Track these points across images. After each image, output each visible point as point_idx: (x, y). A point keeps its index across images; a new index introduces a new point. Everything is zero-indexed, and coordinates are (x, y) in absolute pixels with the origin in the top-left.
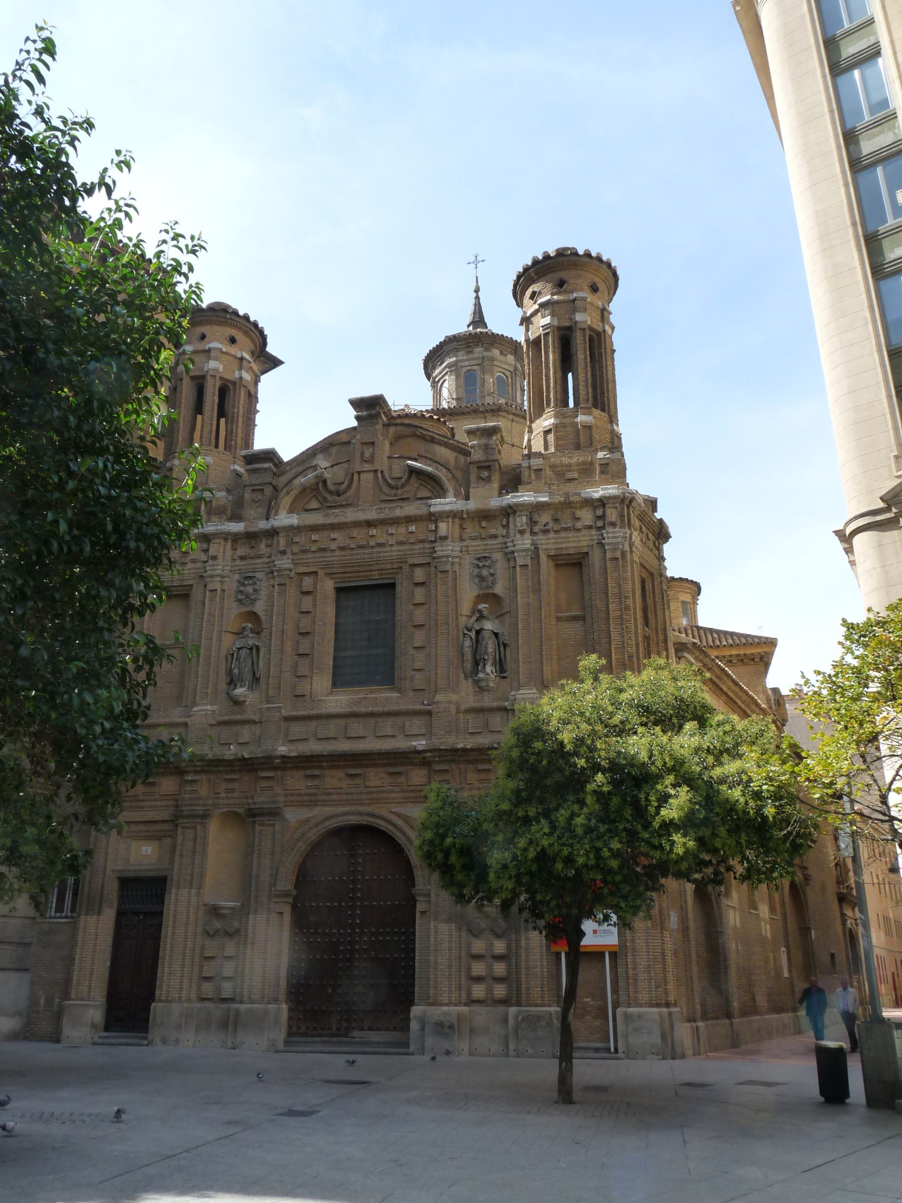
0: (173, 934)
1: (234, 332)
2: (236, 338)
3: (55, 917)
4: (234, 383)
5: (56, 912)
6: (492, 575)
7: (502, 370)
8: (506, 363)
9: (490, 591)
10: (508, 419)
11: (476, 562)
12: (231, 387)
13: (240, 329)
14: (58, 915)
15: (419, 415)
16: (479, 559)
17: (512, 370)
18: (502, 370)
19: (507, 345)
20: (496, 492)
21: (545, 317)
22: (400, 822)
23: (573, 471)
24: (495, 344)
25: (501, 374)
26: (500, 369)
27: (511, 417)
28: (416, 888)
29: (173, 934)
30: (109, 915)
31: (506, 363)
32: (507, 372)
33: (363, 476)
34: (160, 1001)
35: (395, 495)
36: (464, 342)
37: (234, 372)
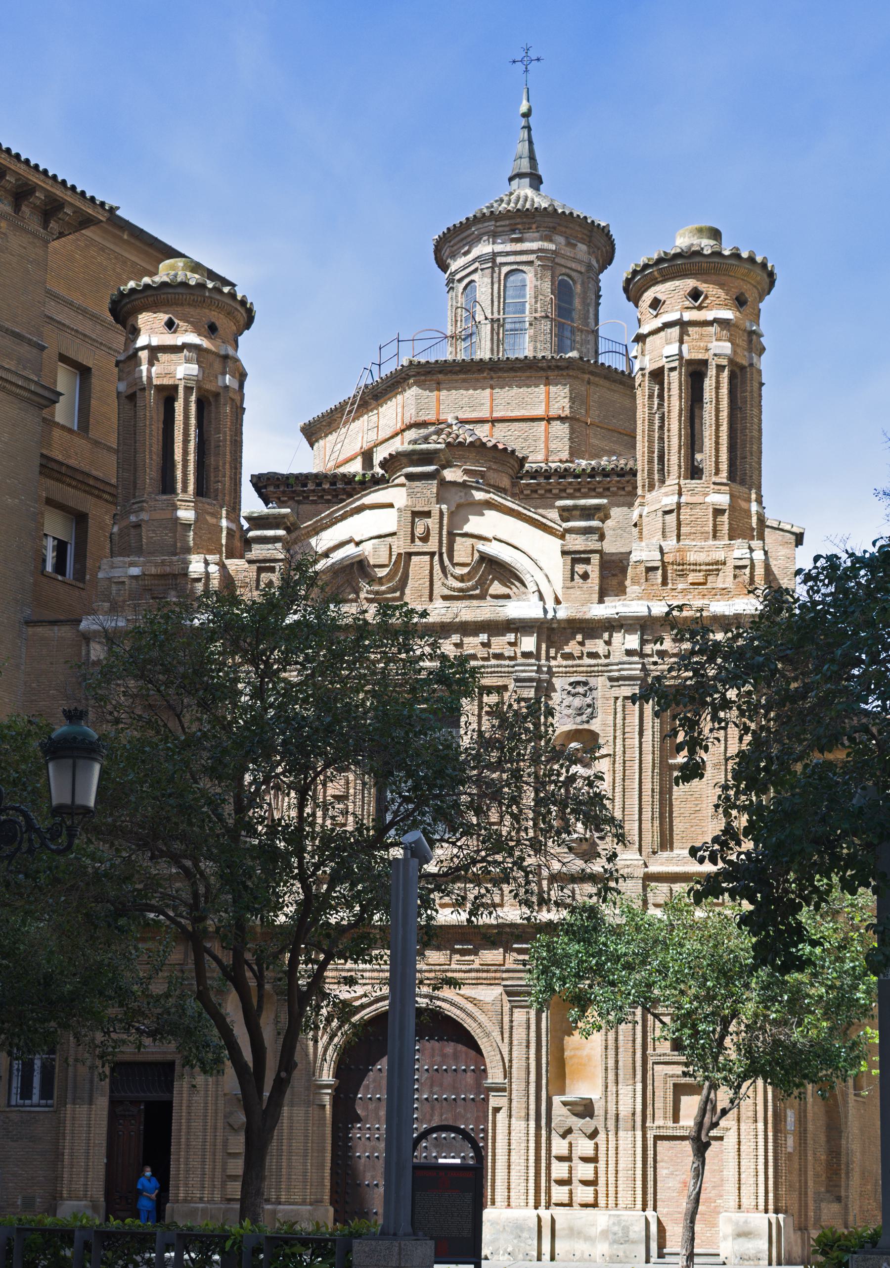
0: (189, 1127)
1: (215, 316)
2: (217, 324)
3: (39, 1106)
4: (217, 395)
5: (42, 1097)
6: (589, 706)
7: (568, 271)
8: (574, 259)
9: (586, 726)
10: (583, 381)
11: (570, 688)
12: (211, 399)
13: (220, 307)
14: (43, 1102)
15: (478, 443)
16: (571, 684)
17: (583, 270)
18: (568, 271)
19: (577, 228)
20: (596, 596)
21: (670, 343)
22: (469, 1006)
23: (700, 571)
24: (559, 228)
25: (566, 278)
26: (564, 270)
27: (586, 376)
28: (489, 1081)
29: (189, 1127)
30: (102, 1103)
31: (574, 259)
32: (573, 274)
33: (414, 559)
34: (177, 1201)
35: (461, 590)
36: (507, 222)
37: (216, 378)
